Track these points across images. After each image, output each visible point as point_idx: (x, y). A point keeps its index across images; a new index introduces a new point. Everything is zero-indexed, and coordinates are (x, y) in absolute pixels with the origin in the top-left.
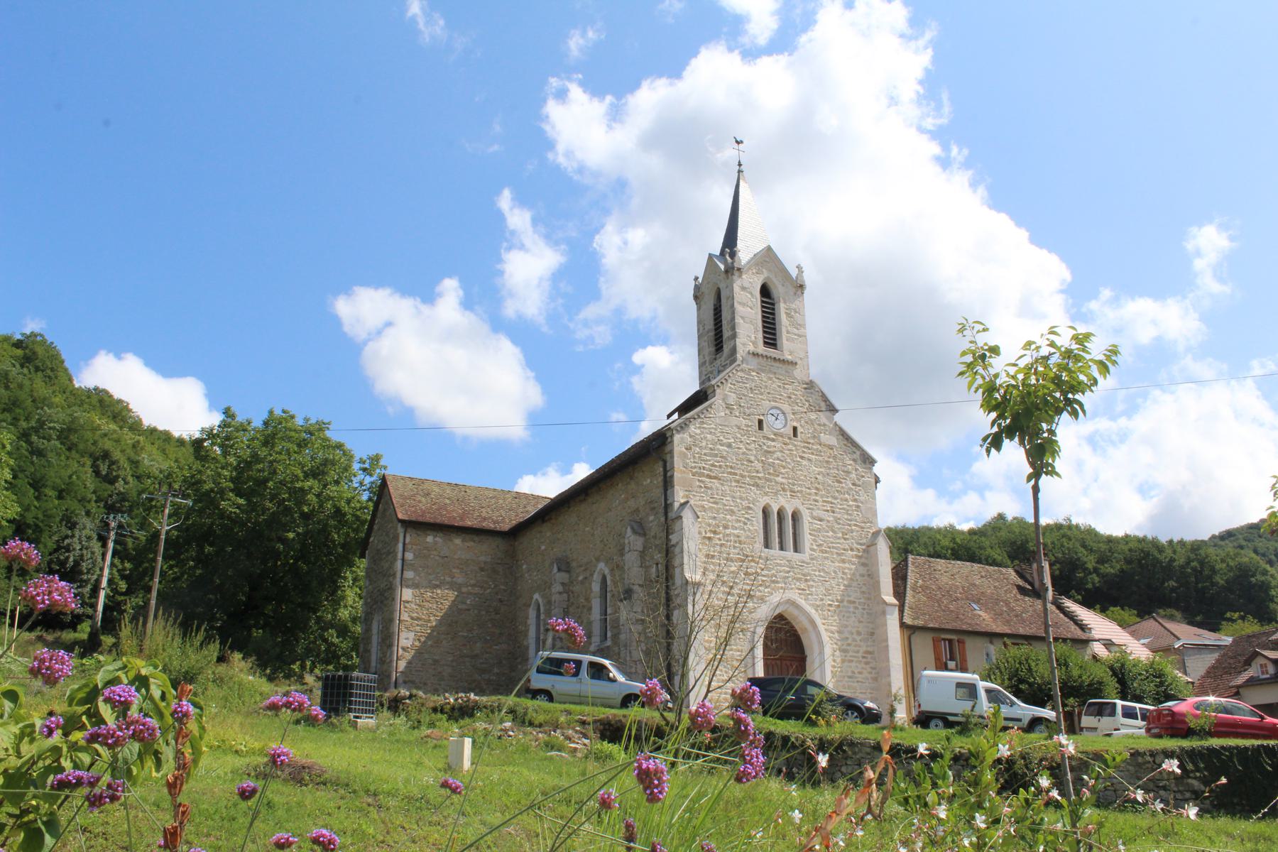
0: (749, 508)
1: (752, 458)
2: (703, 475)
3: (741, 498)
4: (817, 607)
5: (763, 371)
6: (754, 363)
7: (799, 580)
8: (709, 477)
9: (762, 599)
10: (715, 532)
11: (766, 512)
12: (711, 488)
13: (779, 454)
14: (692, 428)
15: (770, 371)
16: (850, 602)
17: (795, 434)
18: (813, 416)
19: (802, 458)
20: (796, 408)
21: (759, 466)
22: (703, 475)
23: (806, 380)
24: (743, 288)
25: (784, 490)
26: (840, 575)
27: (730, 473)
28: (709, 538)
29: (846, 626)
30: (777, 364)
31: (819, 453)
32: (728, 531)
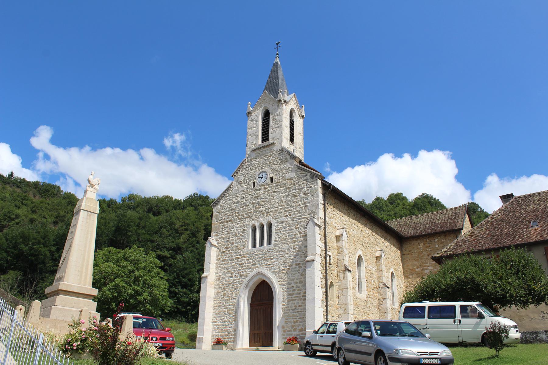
0: (244, 230)
1: (248, 204)
2: (224, 222)
3: (241, 227)
4: (275, 273)
5: (258, 156)
6: (254, 154)
7: (267, 260)
8: (227, 222)
9: (247, 276)
10: (227, 248)
11: (254, 229)
12: (227, 227)
13: (262, 196)
14: (221, 201)
15: (262, 154)
16: (296, 265)
17: (272, 181)
19: (274, 192)
21: (251, 206)
22: (224, 222)
23: (280, 149)
24: (252, 120)
25: (263, 214)
26: (291, 250)
27: (237, 216)
28: (224, 252)
29: (293, 280)
31: (285, 185)
32: (233, 246)
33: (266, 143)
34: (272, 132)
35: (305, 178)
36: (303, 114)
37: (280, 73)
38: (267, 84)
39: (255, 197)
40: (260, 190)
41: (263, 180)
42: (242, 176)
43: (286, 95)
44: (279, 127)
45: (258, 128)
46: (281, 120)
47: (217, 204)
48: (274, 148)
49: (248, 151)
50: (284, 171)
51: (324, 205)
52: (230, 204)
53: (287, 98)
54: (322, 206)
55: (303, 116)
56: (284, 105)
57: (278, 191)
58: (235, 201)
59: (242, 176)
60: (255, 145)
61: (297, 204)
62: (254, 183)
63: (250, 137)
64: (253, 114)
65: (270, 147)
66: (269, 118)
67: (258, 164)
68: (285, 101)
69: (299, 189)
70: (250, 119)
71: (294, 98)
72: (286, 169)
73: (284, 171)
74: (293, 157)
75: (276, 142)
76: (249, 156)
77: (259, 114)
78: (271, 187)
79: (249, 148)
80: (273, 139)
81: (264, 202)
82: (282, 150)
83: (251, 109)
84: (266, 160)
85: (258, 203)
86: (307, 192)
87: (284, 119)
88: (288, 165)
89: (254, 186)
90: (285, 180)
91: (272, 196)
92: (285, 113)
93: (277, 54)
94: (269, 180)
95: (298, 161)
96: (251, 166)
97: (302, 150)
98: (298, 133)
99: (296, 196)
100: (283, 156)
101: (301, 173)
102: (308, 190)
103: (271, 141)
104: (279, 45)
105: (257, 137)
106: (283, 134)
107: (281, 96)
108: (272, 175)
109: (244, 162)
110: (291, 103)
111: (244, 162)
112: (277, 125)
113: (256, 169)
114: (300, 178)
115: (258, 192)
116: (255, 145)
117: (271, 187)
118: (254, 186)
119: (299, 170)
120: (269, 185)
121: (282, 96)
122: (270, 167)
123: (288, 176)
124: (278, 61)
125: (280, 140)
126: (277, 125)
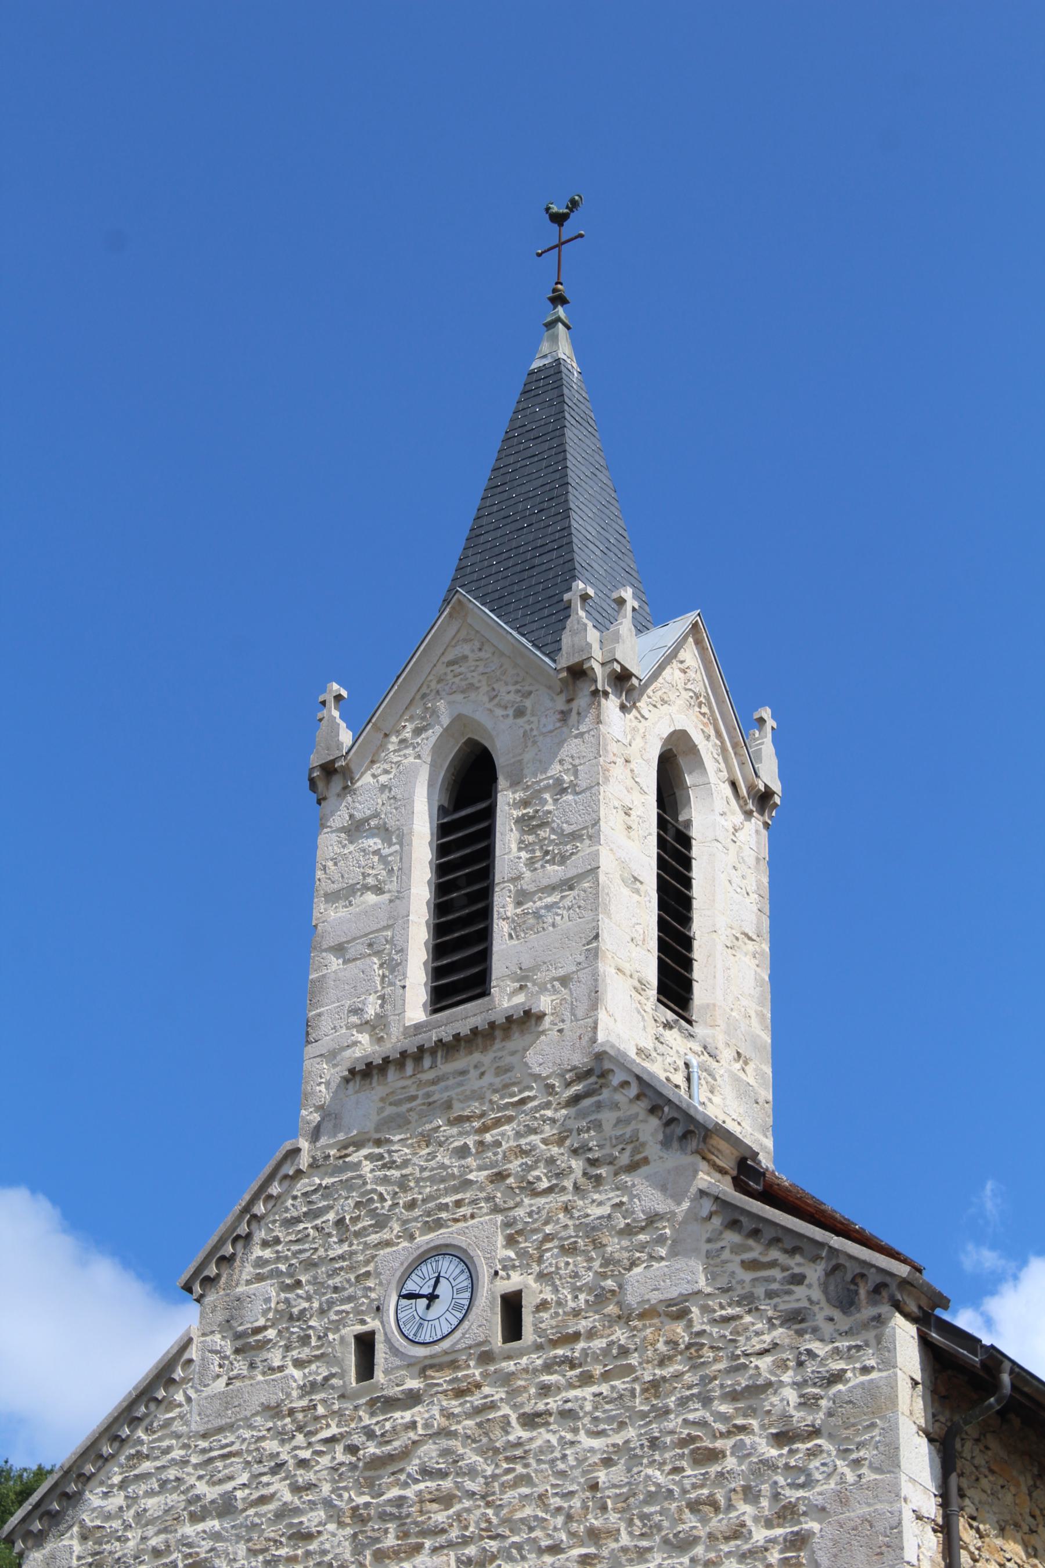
1: (312, 1519)
5: (400, 1122)
6: (367, 1106)
13: (429, 1452)
14: (94, 1498)
17: (513, 1329)
18: (596, 1207)
19: (531, 1420)
20: (525, 1208)
23: (579, 1059)
24: (356, 829)
30: (462, 1062)
33: (466, 1017)
34: (518, 928)
35: (788, 1304)
36: (769, 776)
37: (581, 447)
38: (474, 537)
39: (377, 1463)
40: (413, 1399)
41: (441, 1316)
42: (270, 1289)
43: (625, 625)
44: (568, 884)
45: (401, 896)
46: (589, 831)
47: (54, 1518)
48: (532, 1058)
49: (322, 1079)
50: (614, 1245)
51: (946, 1529)
52: (168, 1522)
53: (634, 650)
54: (933, 1542)
55: (764, 799)
56: (611, 705)
57: (567, 1415)
58: (210, 1493)
59: (270, 1289)
60: (376, 1027)
61: (718, 1523)
62: (365, 1344)
63: (335, 963)
64: (366, 781)
65: (501, 1050)
66: (490, 813)
67: (403, 1184)
68: (622, 679)
69: (733, 1396)
70: (340, 818)
71: (690, 655)
72: (628, 1231)
73: (614, 1245)
74: (689, 1131)
75: (545, 1003)
76: (331, 1117)
77: (407, 777)
78: (506, 1379)
79: (331, 1056)
80: (523, 979)
81: (446, 1500)
82: (599, 1074)
83: (346, 737)
84: (463, 1152)
85: (395, 1513)
86: (801, 1419)
87: (611, 823)
88: (647, 1197)
89: (366, 1368)
90: (624, 1318)
91: (516, 1453)
92: (618, 772)
93: (559, 299)
94: (488, 1322)
95: (728, 1163)
96: (346, 1205)
97: (759, 1075)
98: (724, 937)
99: (714, 1456)
100: (608, 1117)
101: (752, 1265)
102: (808, 1403)
103: (505, 997)
104: (569, 228)
105: (394, 967)
106: (607, 942)
107: (587, 638)
108: (515, 1281)
109: (284, 1169)
110: (668, 690)
111: (284, 1169)
112: (555, 872)
113: (381, 1223)
114: (749, 1302)
115: (403, 1416)
116: (376, 1027)
117: (506, 1379)
118: (366, 1368)
119: (733, 1237)
120: (486, 1358)
121: (593, 636)
122: (492, 1211)
123: (644, 1284)
124: (564, 350)
125: (580, 990)
126: (555, 872)
